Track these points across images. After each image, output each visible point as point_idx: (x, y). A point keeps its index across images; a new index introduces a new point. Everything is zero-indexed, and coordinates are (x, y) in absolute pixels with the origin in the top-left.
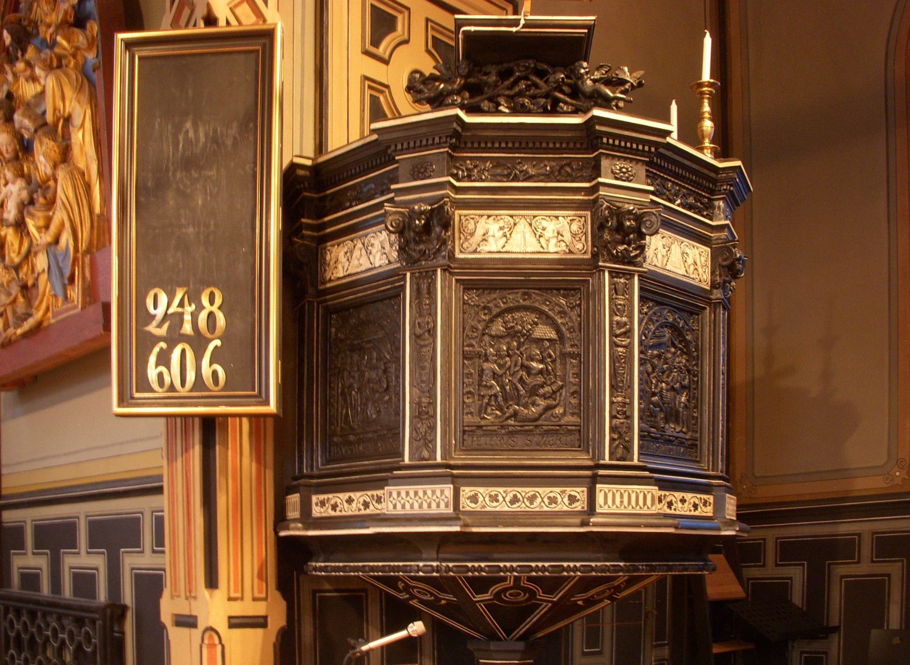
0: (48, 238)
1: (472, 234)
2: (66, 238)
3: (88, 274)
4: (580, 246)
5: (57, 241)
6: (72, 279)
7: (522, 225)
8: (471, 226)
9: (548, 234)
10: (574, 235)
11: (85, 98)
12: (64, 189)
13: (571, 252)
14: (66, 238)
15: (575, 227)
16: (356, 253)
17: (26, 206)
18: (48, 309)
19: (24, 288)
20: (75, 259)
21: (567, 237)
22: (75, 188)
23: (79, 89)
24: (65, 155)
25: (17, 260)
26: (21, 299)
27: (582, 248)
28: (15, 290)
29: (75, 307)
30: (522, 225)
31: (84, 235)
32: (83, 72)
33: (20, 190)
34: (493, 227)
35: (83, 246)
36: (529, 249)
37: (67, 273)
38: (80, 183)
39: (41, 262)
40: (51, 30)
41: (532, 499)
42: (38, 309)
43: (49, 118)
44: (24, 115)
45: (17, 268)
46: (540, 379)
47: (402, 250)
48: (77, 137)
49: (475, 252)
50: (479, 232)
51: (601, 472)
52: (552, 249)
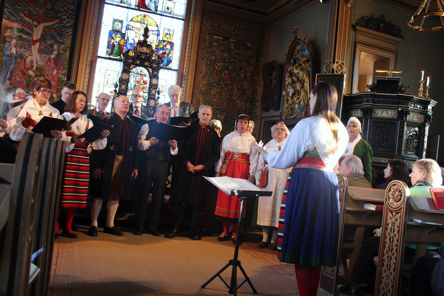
0: (298, 102)
1: (376, 113)
2: (302, 103)
3: (306, 110)
4: (395, 116)
5: (300, 102)
6: (303, 111)
7: (385, 112)
8: (376, 111)
9: (389, 114)
10: (394, 114)
11: (308, 77)
12: (302, 93)
13: (393, 117)
14: (302, 103)
15: (394, 113)
16: (356, 113)
17: (293, 94)
18: (297, 115)
19: (291, 109)
20: (304, 107)
21: (393, 114)
22: (305, 94)
23: (307, 75)
24: (303, 87)
25: (291, 104)
26: (290, 111)
27: (395, 116)
28: (289, 109)
29: (303, 116)
30: (385, 112)
31: (306, 102)
32: (307, 72)
33: (293, 91)
34: (380, 112)
35: (305, 104)
36: (386, 116)
37: (302, 109)
38: (306, 93)
39: (297, 106)
40: (302, 62)
41: (382, 160)
42: (295, 114)
43: (300, 79)
44: (295, 78)
45: (291, 105)
46: (385, 139)
47: (363, 114)
48: (306, 84)
49: (376, 116)
50: (377, 112)
51: (395, 157)
52: (390, 116)
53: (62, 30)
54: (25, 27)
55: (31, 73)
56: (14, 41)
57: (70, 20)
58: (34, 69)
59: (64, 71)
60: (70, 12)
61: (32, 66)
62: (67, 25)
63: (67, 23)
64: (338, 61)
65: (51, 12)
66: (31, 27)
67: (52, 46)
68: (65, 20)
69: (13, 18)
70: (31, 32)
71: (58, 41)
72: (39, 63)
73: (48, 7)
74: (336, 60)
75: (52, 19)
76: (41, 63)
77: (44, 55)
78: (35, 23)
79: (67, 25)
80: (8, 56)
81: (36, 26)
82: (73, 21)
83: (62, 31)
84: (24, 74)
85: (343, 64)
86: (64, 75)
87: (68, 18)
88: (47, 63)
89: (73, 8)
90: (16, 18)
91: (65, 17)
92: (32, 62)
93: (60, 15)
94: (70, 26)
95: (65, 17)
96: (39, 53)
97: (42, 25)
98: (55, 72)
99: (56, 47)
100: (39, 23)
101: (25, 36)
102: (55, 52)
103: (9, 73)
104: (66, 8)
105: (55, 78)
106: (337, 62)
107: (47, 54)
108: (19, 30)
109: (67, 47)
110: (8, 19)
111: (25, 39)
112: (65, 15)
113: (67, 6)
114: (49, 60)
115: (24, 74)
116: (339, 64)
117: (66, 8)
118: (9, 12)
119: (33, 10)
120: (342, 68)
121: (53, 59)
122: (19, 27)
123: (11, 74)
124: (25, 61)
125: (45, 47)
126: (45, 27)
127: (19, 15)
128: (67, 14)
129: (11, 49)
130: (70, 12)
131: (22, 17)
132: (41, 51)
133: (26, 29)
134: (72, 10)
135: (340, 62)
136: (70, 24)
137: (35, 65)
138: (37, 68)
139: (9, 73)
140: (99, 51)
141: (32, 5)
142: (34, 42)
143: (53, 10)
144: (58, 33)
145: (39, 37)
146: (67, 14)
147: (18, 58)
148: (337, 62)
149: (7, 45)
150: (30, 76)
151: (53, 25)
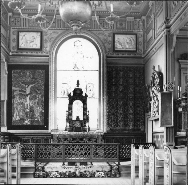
53: (39, 87)
54: (22, 88)
55: (28, 110)
56: (18, 96)
57: (42, 82)
58: (29, 108)
59: (43, 107)
60: (42, 77)
61: (28, 107)
62: (42, 84)
63: (41, 83)
64: (169, 82)
65: (33, 79)
66: (25, 88)
67: (35, 96)
68: (40, 82)
69: (17, 86)
70: (25, 91)
71: (38, 93)
72: (31, 105)
73: (31, 77)
74: (168, 82)
75: (34, 83)
76: (31, 105)
77: (32, 101)
78: (27, 86)
79: (42, 84)
80: (17, 104)
81: (27, 88)
82: (44, 82)
83: (40, 88)
84: (25, 111)
85: (172, 83)
86: (43, 109)
87: (41, 81)
88: (34, 104)
89: (43, 75)
90: (18, 85)
91: (40, 80)
92: (27, 105)
93: (37, 80)
94: (43, 85)
95: (40, 80)
96: (30, 100)
97: (30, 86)
98: (38, 108)
99: (37, 96)
100: (28, 86)
101: (23, 93)
102: (38, 99)
103: (18, 112)
104: (40, 76)
105: (39, 112)
106: (169, 83)
107: (34, 100)
108: (20, 91)
109: (43, 95)
110: (15, 87)
111: (23, 94)
112: (40, 79)
113: (40, 75)
114: (35, 103)
115: (25, 111)
116: (170, 84)
117: (40, 76)
118: (15, 83)
119: (25, 80)
120: (172, 86)
121: (37, 102)
122: (20, 89)
123: (19, 112)
124: (24, 105)
125: (33, 97)
126: (31, 87)
127: (19, 84)
128: (41, 79)
129: (17, 101)
130: (42, 77)
131: (20, 84)
132: (30, 99)
133: (23, 90)
134: (43, 77)
135: (170, 83)
136: (43, 84)
137: (29, 106)
138: (30, 108)
139: (18, 112)
140: (57, 96)
141: (24, 78)
142: (27, 95)
143: (33, 78)
144: (38, 89)
145: (29, 92)
146: (41, 79)
147: (21, 104)
148: (169, 83)
149: (15, 99)
150: (27, 112)
151: (34, 86)
